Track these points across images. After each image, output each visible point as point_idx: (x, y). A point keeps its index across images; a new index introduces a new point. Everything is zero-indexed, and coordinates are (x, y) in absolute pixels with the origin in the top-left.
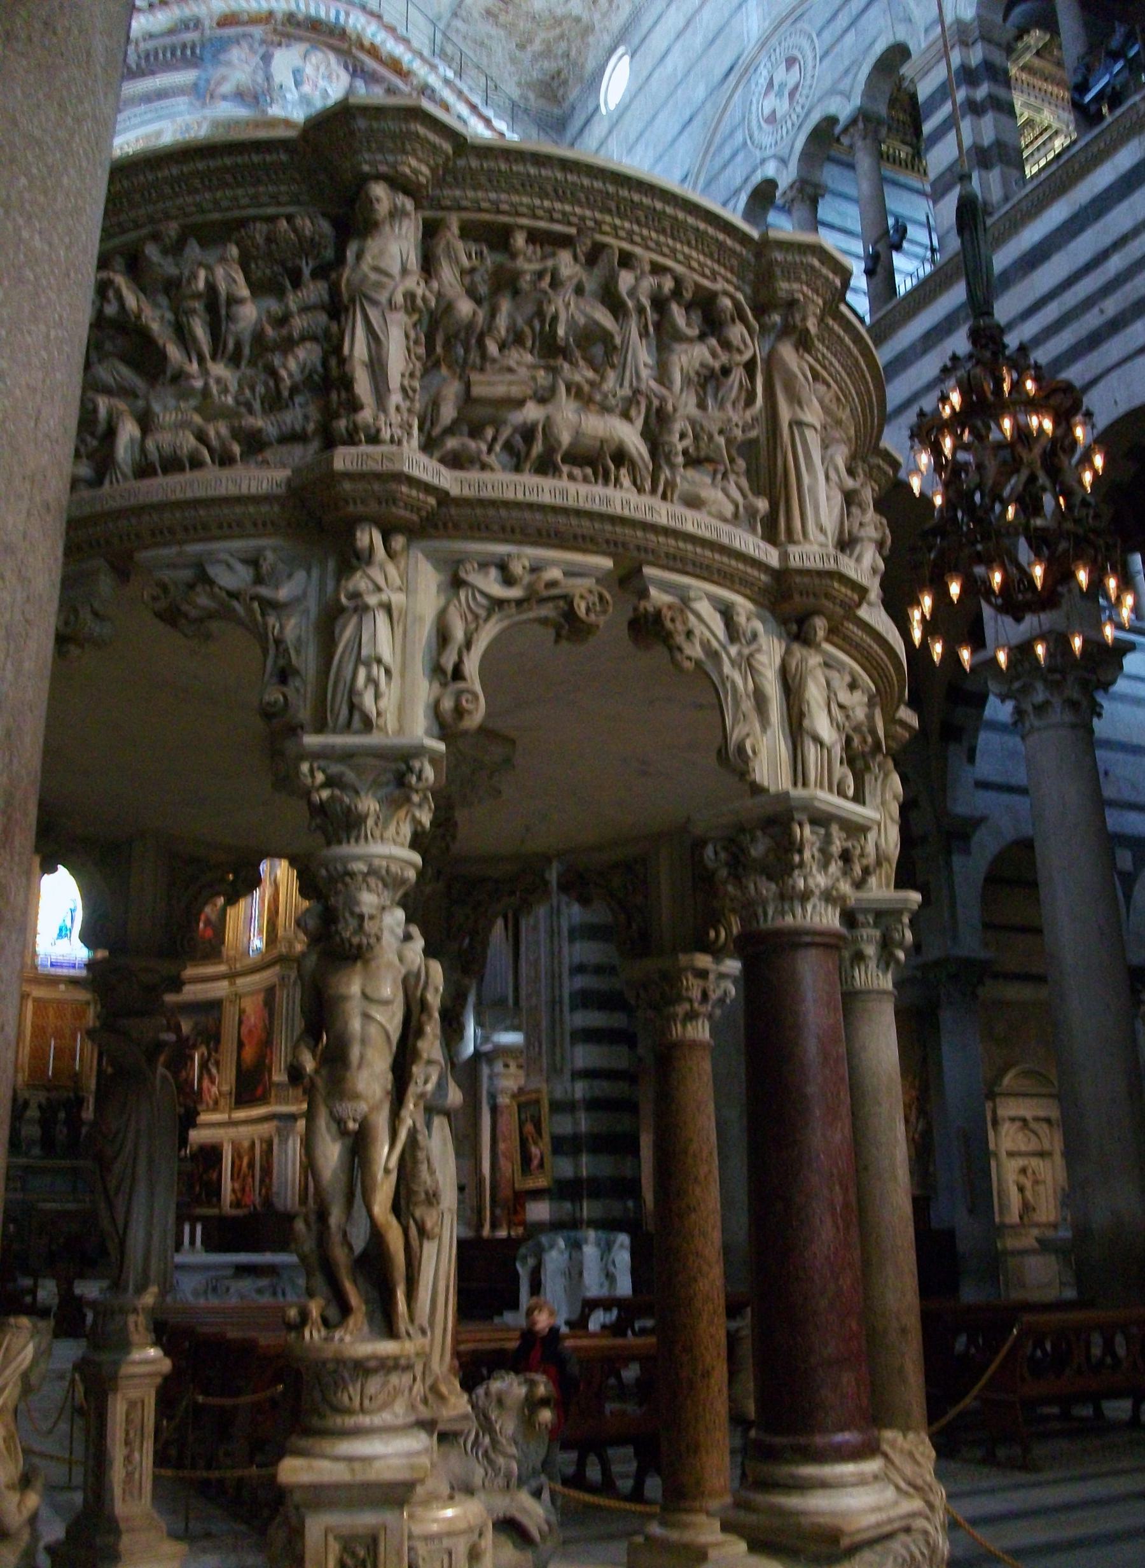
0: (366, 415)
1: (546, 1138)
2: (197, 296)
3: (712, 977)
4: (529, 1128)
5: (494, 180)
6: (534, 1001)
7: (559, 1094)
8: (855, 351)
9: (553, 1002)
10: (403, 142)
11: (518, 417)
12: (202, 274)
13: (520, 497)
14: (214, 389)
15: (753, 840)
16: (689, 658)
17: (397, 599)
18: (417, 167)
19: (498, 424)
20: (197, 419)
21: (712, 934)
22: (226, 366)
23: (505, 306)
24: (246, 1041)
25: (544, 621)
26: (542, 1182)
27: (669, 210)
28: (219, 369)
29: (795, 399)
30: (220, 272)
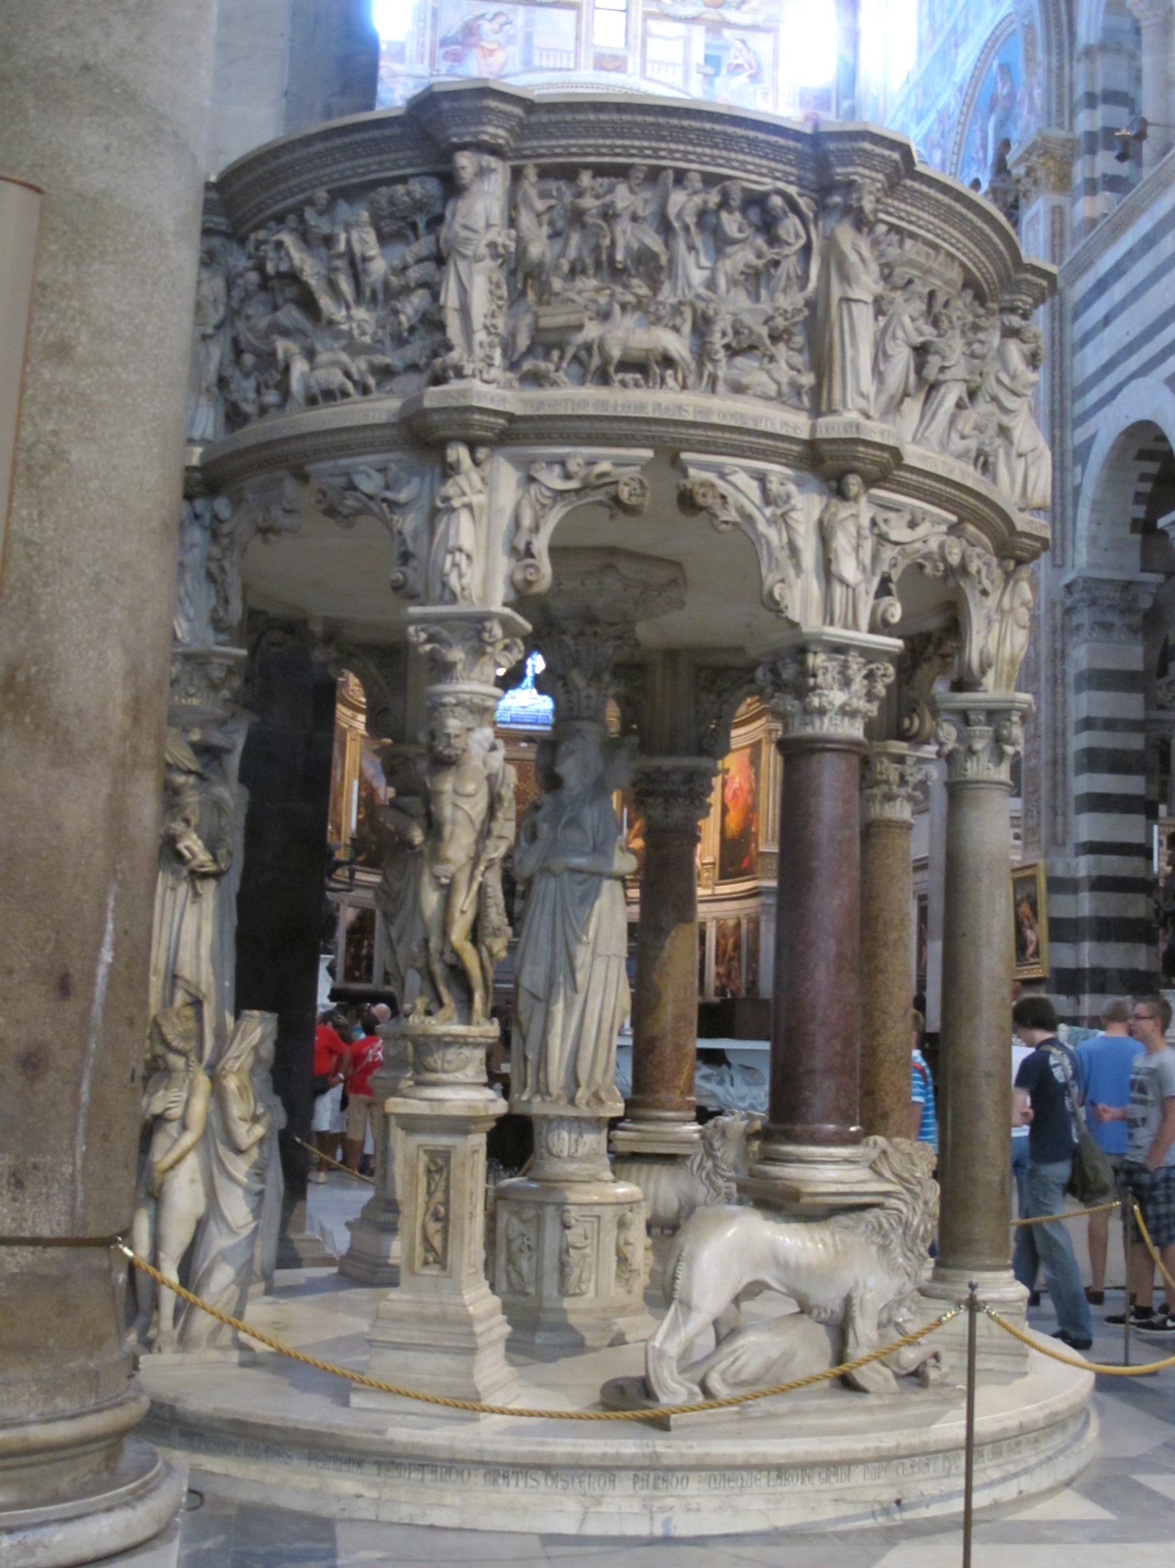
0: (454, 356)
1: (1043, 922)
2: (340, 256)
3: (910, 761)
4: (1025, 908)
5: (565, 129)
6: (1033, 762)
7: (1060, 871)
8: (946, 200)
9: (1054, 763)
10: (480, 116)
11: (579, 338)
12: (343, 237)
13: (569, 412)
14: (356, 332)
15: (785, 665)
16: (726, 522)
17: (477, 499)
18: (495, 133)
19: (561, 347)
20: (344, 357)
21: (907, 723)
22: (368, 309)
23: (575, 239)
24: (730, 805)
25: (600, 503)
26: (1037, 972)
27: (718, 127)
28: (360, 313)
29: (845, 279)
30: (355, 235)
